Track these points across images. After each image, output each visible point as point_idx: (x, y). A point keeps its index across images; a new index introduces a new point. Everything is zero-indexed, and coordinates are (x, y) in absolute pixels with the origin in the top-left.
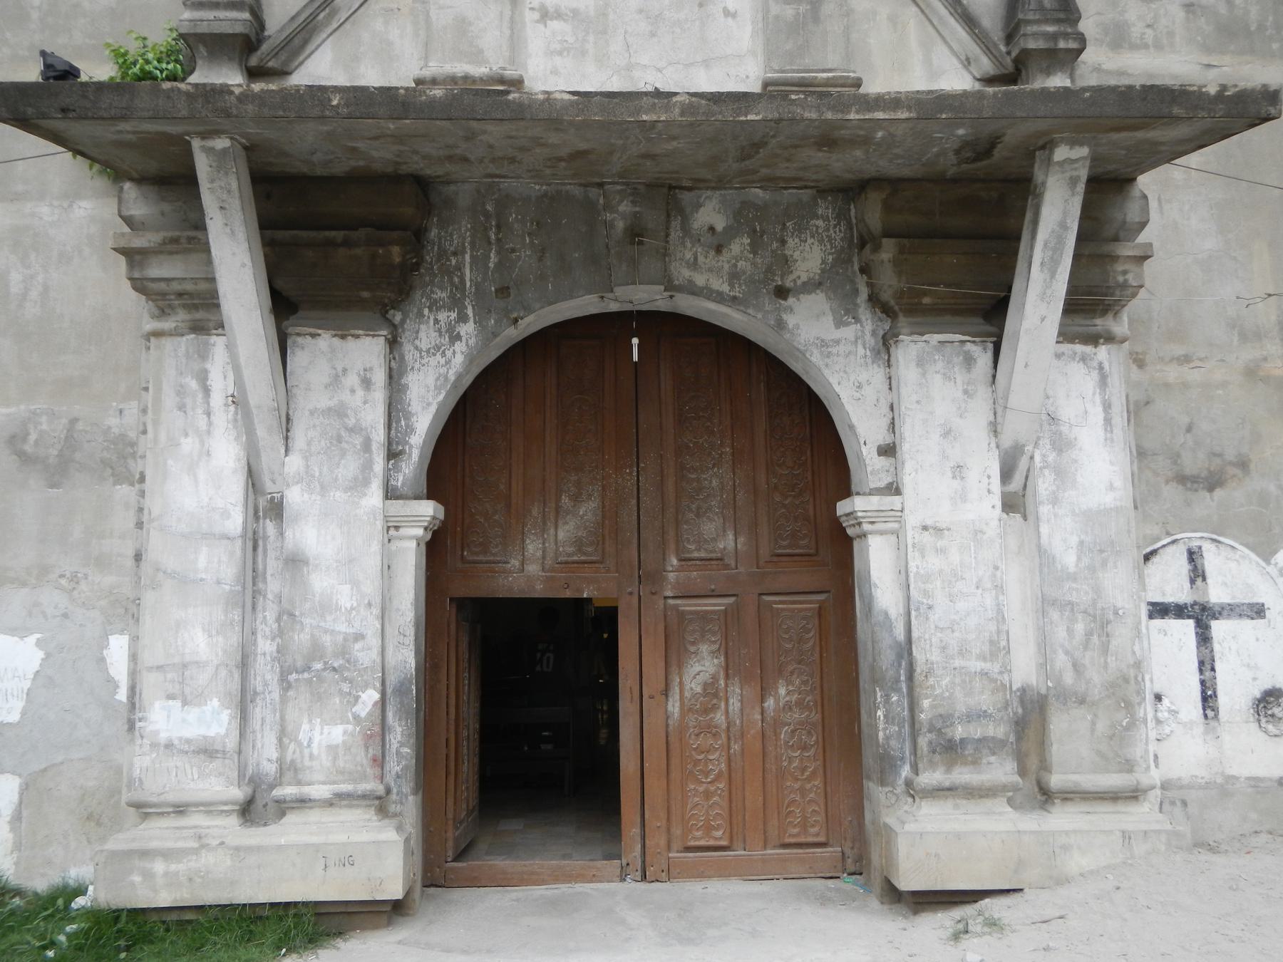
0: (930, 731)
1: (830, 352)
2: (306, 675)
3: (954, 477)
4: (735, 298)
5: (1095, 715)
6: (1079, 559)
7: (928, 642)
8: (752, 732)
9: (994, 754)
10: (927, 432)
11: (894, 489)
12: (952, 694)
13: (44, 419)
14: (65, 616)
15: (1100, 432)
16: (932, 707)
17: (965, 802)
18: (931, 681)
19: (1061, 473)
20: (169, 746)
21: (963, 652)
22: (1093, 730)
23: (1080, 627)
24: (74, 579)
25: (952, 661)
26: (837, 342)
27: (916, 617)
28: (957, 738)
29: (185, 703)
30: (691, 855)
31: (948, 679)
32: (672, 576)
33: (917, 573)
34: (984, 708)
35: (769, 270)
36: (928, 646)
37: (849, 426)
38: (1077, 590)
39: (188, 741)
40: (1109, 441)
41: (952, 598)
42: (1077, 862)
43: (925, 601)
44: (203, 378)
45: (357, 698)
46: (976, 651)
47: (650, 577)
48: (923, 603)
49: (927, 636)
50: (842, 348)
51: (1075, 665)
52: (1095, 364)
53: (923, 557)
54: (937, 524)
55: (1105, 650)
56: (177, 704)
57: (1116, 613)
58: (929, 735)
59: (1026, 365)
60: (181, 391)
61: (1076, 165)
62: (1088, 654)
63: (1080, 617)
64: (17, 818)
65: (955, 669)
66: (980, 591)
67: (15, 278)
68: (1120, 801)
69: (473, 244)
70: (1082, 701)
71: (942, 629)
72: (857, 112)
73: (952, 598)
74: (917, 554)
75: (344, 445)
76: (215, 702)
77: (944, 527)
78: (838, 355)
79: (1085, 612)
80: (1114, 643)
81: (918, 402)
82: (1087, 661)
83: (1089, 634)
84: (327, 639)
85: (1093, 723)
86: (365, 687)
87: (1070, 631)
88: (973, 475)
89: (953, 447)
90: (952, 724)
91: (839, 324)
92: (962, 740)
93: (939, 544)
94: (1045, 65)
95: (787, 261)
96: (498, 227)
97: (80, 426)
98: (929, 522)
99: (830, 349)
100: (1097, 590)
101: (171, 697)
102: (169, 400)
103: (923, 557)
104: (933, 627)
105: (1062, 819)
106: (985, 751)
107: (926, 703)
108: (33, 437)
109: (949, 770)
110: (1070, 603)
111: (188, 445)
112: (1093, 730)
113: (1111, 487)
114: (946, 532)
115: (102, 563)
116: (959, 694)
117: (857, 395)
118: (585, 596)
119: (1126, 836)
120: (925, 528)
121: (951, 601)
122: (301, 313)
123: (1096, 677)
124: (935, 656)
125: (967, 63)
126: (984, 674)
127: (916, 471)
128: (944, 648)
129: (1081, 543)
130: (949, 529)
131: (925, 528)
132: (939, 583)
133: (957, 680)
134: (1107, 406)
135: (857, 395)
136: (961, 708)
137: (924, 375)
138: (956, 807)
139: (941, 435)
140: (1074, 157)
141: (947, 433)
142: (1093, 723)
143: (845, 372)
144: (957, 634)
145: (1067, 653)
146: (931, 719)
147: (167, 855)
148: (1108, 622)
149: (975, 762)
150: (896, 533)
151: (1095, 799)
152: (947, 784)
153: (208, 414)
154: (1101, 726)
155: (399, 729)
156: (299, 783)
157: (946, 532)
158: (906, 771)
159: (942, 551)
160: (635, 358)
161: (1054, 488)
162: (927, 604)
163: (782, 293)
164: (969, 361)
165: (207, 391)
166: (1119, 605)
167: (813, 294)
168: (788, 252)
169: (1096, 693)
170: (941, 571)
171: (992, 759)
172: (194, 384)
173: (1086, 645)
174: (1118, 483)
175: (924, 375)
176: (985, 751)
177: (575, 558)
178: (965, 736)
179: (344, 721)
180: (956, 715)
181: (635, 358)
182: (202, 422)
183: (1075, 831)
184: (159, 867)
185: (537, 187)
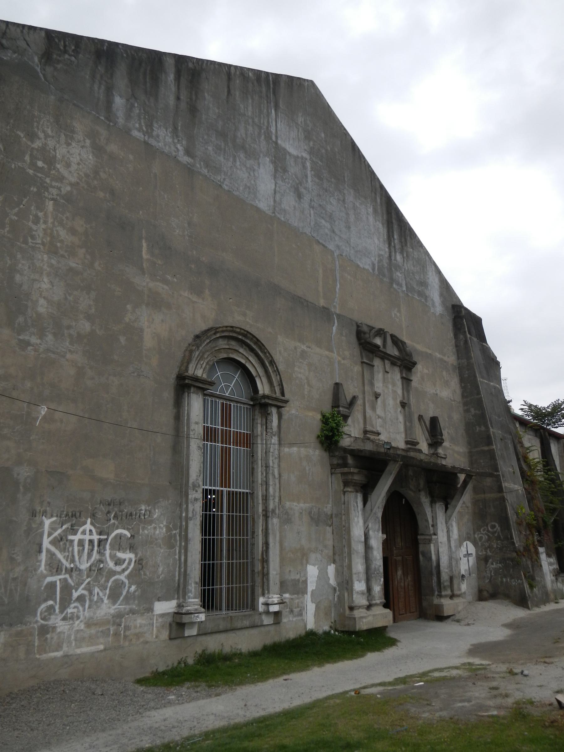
11: (435, 534)
13: (314, 508)
14: (321, 561)
19: (452, 532)
20: (358, 592)
24: (322, 551)
29: (359, 582)
32: (395, 551)
37: (425, 520)
39: (360, 591)
42: (460, 608)
44: (357, 503)
56: (358, 582)
60: (354, 506)
64: (315, 615)
67: (307, 468)
76: (363, 582)
84: (376, 566)
86: (381, 578)
91: (426, 498)
97: (320, 510)
101: (357, 580)
102: (353, 508)
105: (456, 600)
107: (442, 578)
108: (313, 513)
111: (356, 519)
115: (325, 546)
125: (427, 440)
147: (365, 617)
150: (434, 543)
153: (358, 512)
156: (375, 600)
158: (436, 593)
163: (420, 491)
164: (443, 508)
165: (357, 506)
172: (356, 505)
182: (357, 514)
184: (364, 620)
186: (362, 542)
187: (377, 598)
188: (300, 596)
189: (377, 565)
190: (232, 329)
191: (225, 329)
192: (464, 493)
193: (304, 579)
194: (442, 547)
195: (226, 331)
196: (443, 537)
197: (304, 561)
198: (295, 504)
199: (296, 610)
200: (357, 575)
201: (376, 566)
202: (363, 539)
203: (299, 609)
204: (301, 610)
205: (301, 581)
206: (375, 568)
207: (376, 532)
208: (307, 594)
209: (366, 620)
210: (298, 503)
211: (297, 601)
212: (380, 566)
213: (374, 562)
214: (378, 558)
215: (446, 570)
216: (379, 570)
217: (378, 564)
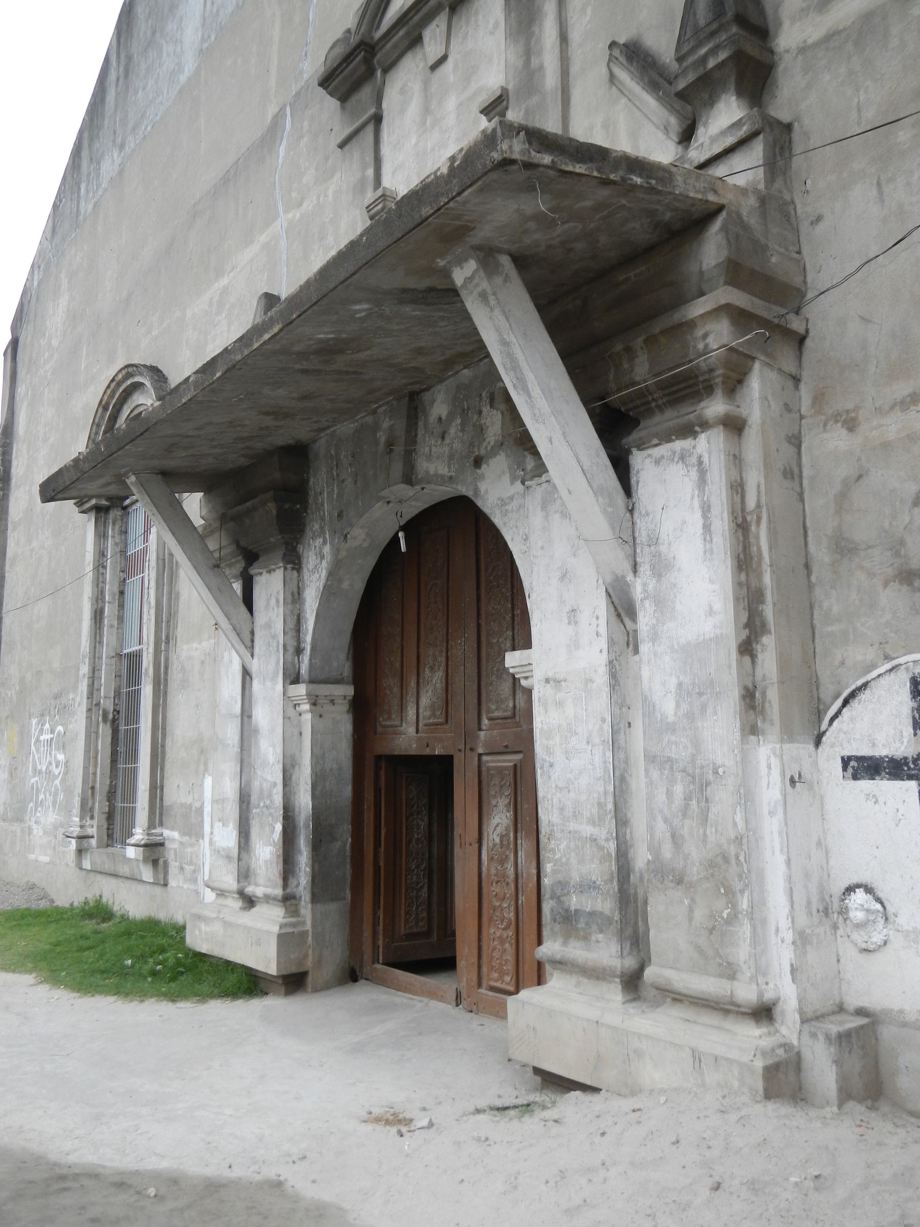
0: (552, 898)
1: (506, 510)
2: (258, 810)
3: (569, 623)
4: (451, 477)
5: (693, 900)
6: (678, 705)
7: (550, 802)
8: (530, 885)
9: (601, 931)
10: (549, 578)
12: (568, 860)
15: (699, 544)
16: (554, 872)
17: (586, 981)
18: (552, 844)
19: (660, 603)
21: (576, 815)
22: (690, 919)
23: (679, 790)
25: (568, 824)
26: (511, 498)
27: (541, 775)
28: (573, 908)
30: (491, 993)
31: (565, 843)
33: (542, 729)
34: (594, 878)
35: (472, 444)
36: (550, 807)
38: (676, 743)
39: (224, 849)
40: (708, 552)
41: (568, 755)
43: (547, 758)
45: (274, 828)
46: (587, 814)
47: (469, 737)
48: (545, 761)
49: (549, 797)
50: (514, 505)
51: (673, 836)
52: (694, 460)
53: (546, 712)
54: (557, 676)
55: (704, 819)
56: (221, 824)
57: (716, 772)
58: (551, 902)
59: (570, 492)
61: (476, 281)
62: (687, 822)
63: (679, 776)
65: (570, 832)
66: (589, 747)
68: (731, 1016)
69: (327, 484)
70: (679, 882)
71: (560, 788)
72: (257, 342)
73: (568, 755)
74: (542, 709)
75: (271, 649)
76: (231, 825)
77: (562, 678)
78: (512, 511)
79: (684, 771)
80: (714, 810)
81: (542, 548)
82: (685, 832)
83: (688, 798)
85: (691, 910)
87: (669, 794)
88: (584, 617)
89: (568, 590)
90: (568, 893)
92: (576, 911)
93: (559, 695)
94: (706, 96)
95: (482, 430)
96: (337, 466)
98: (550, 674)
99: (507, 507)
100: (696, 743)
101: (220, 820)
103: (546, 712)
104: (554, 786)
106: (594, 927)
109: (565, 943)
110: (669, 760)
112: (690, 919)
113: (711, 612)
114: (563, 683)
116: (574, 861)
117: (524, 548)
118: (437, 753)
119: (697, 1057)
120: (547, 681)
121: (567, 758)
122: (261, 559)
123: (695, 853)
124: (555, 818)
126: (594, 840)
127: (541, 621)
128: (562, 809)
129: (680, 685)
130: (565, 681)
131: (547, 681)
132: (558, 739)
133: (572, 845)
134: (706, 509)
135: (524, 548)
136: (575, 878)
137: (546, 518)
138: (578, 984)
139: (559, 579)
140: (469, 274)
141: (563, 577)
142: (691, 910)
143: (516, 527)
144: (572, 795)
145: (666, 820)
146: (552, 885)
148: (708, 784)
149: (586, 938)
151: (704, 1006)
152: (558, 957)
154: (700, 914)
155: (305, 854)
156: (257, 885)
157: (563, 683)
159: (560, 704)
160: (403, 548)
161: (654, 621)
162: (550, 762)
166: (719, 761)
167: (498, 456)
168: (483, 422)
169: (694, 872)
170: (559, 726)
171: (600, 937)
173: (685, 812)
174: (718, 606)
175: (546, 518)
176: (594, 927)
177: (431, 721)
178: (579, 907)
179: (270, 845)
180: (572, 884)
181: (403, 548)
183: (646, 1036)
184: (203, 927)
185: (352, 426)
186: (237, 717)
187: (261, 881)
188: (193, 840)
189: (265, 780)
190: (114, 383)
191: (109, 392)
192: (508, 381)
193: (198, 805)
194: (560, 704)
195: (114, 392)
196: (575, 644)
197: (202, 768)
198: (195, 645)
199: (189, 868)
200: (220, 806)
201: (265, 785)
202: (238, 708)
203: (192, 868)
204: (194, 871)
205: (194, 809)
206: (262, 790)
207: (268, 683)
208: (203, 838)
209: (208, 929)
210: (200, 643)
211: (189, 850)
212: (275, 784)
213: (259, 772)
214: (271, 759)
215: (588, 830)
216: (270, 796)
217: (269, 778)
